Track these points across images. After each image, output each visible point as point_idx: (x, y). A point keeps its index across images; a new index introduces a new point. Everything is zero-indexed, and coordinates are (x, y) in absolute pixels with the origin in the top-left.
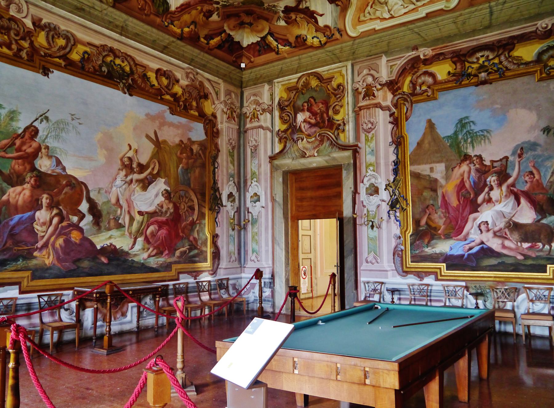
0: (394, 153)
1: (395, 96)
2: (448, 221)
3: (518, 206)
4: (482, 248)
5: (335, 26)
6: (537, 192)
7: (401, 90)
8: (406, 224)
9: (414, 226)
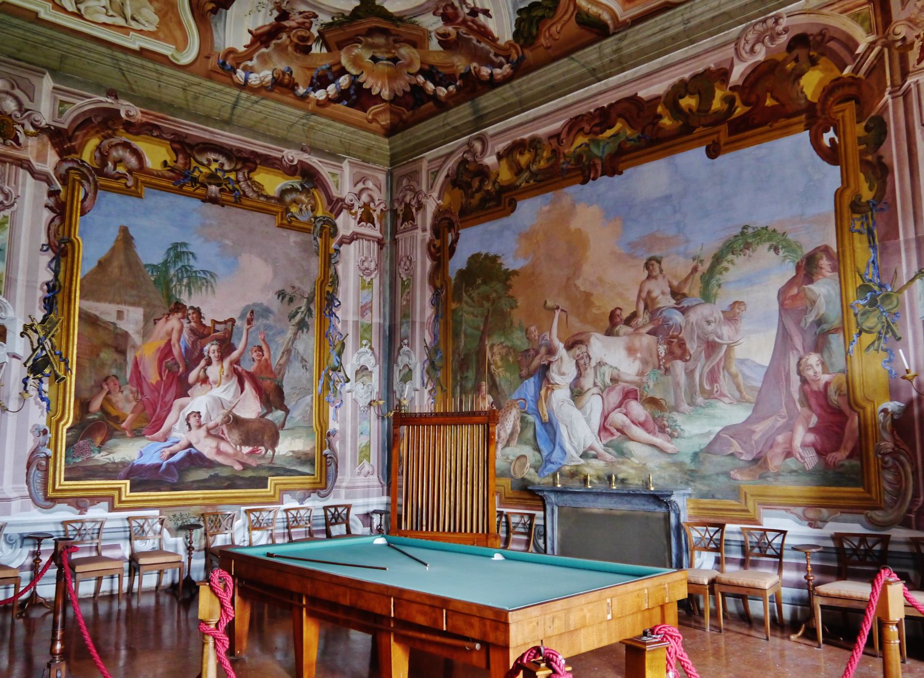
0: (49, 266)
1: (63, 160)
2: (141, 407)
3: (242, 391)
4: (189, 454)
6: (264, 376)
7: (78, 156)
8: (60, 408)
9: (78, 413)
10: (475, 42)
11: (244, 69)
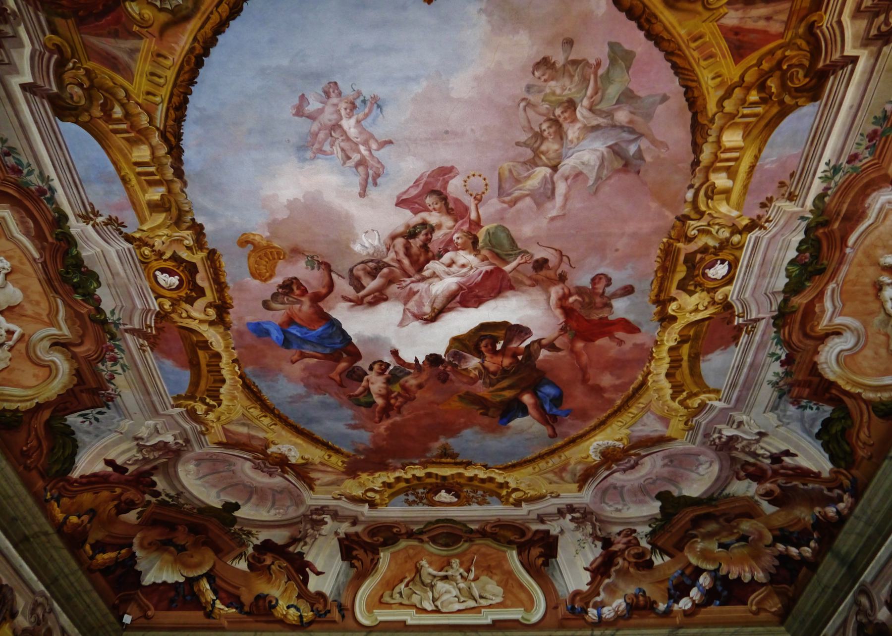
5: (337, 598)
10: (801, 486)
11: (595, 606)
